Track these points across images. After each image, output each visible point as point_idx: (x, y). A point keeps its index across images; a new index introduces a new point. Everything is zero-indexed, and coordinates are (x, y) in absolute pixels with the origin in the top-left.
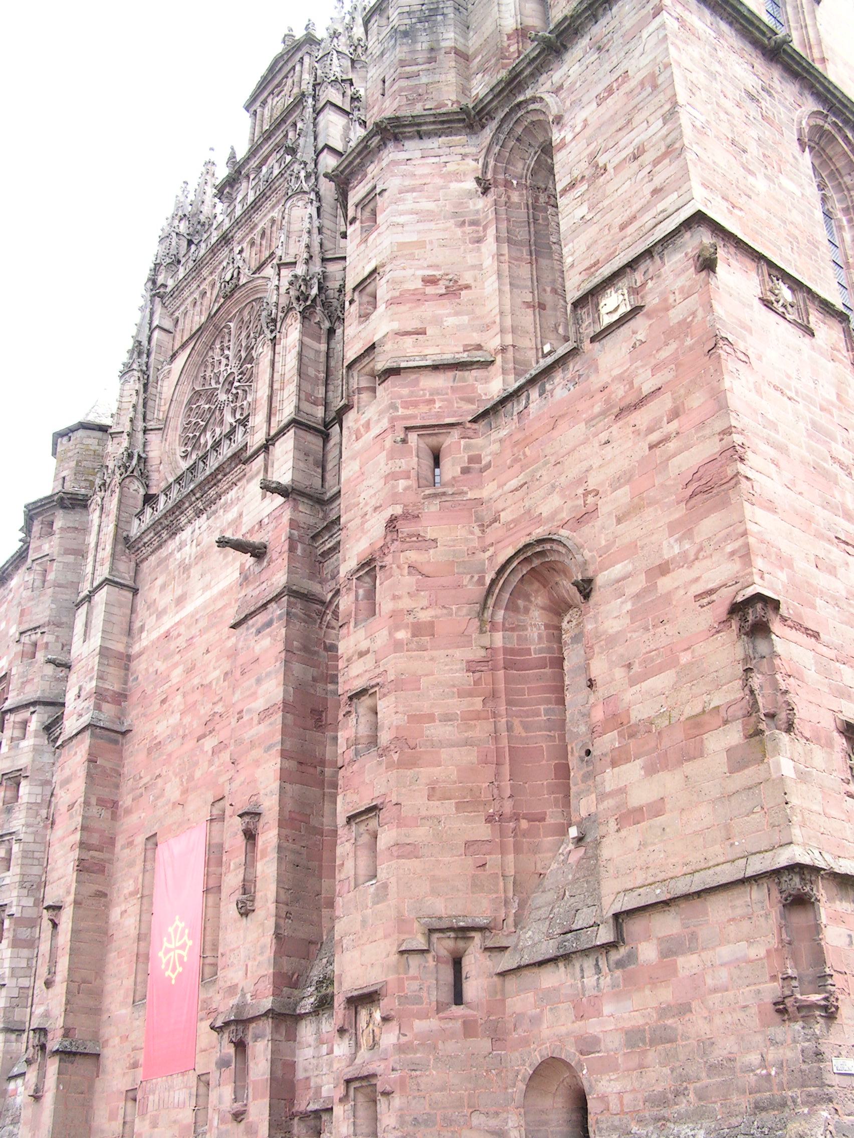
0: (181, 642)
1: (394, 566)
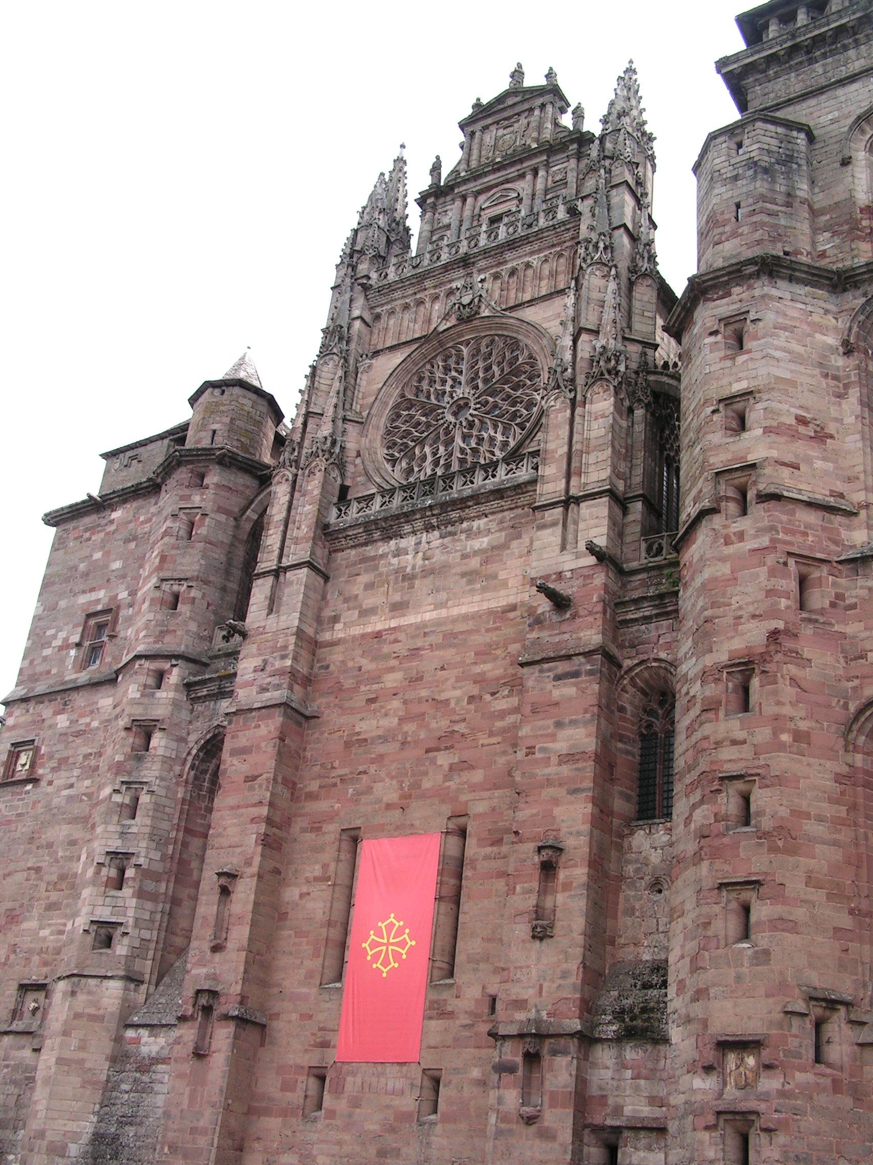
0: (401, 648)
1: (779, 675)
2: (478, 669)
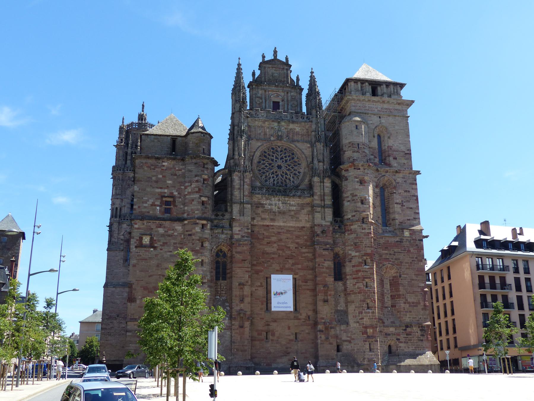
0: (275, 231)
2: (297, 241)
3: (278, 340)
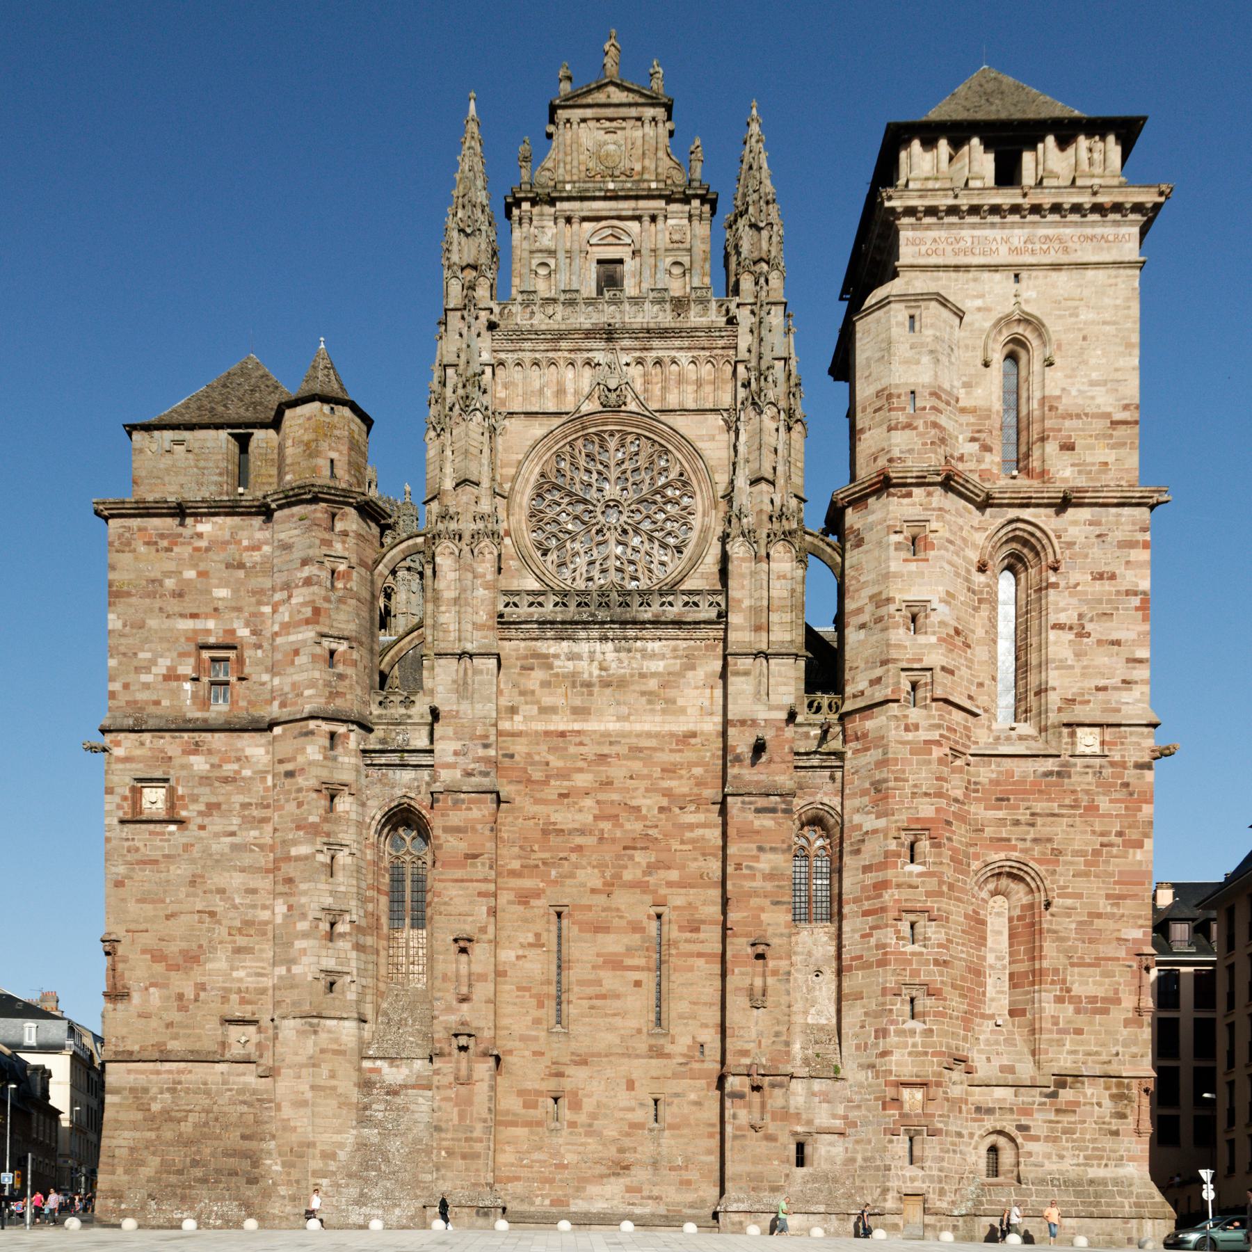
0: (590, 750)
2: (666, 784)
3: (590, 1125)
